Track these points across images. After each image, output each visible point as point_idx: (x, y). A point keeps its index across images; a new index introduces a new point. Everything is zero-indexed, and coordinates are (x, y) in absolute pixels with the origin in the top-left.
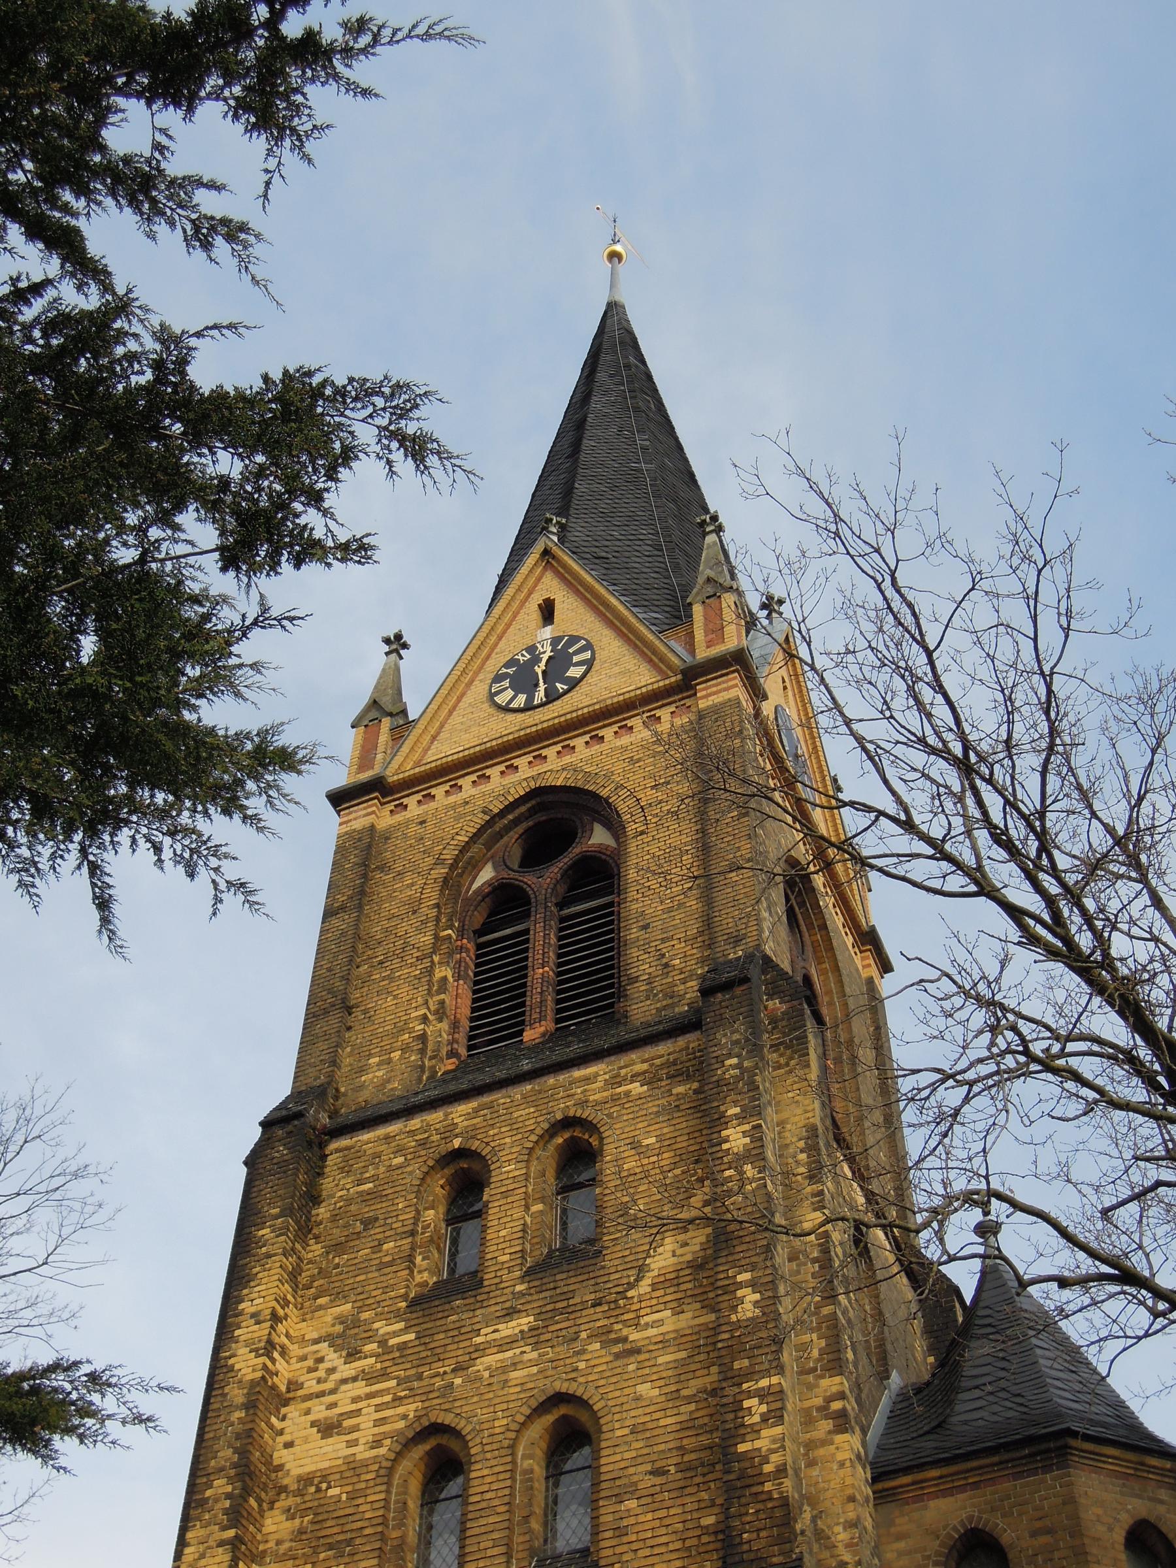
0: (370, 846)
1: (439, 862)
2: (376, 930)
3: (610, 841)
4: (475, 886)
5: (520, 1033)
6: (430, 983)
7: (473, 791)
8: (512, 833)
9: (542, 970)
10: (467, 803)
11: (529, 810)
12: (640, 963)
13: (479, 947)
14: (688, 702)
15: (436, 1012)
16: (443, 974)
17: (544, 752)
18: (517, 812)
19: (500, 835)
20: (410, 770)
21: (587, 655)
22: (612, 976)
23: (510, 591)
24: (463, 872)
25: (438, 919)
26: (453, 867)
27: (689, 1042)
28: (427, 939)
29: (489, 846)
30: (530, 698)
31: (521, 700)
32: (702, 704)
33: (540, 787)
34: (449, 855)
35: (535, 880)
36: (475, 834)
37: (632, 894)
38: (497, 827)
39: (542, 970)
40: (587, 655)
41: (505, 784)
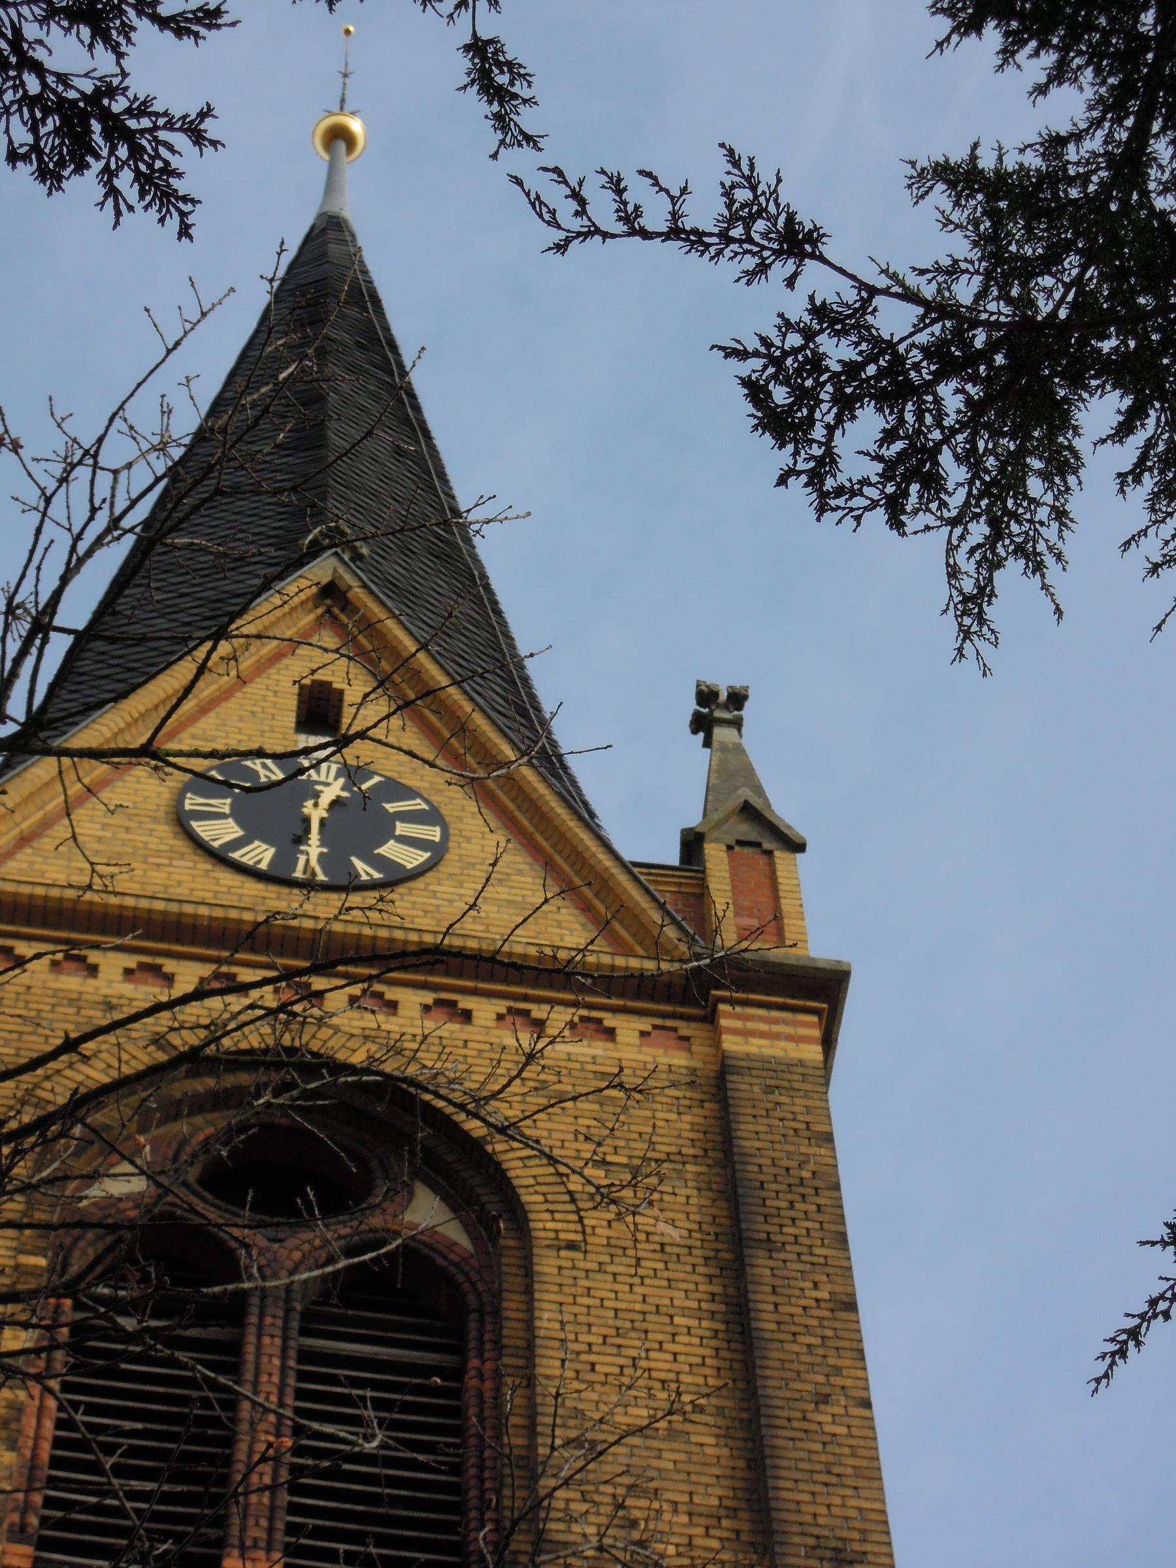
8: (198, 1120)
37: (548, 1366)
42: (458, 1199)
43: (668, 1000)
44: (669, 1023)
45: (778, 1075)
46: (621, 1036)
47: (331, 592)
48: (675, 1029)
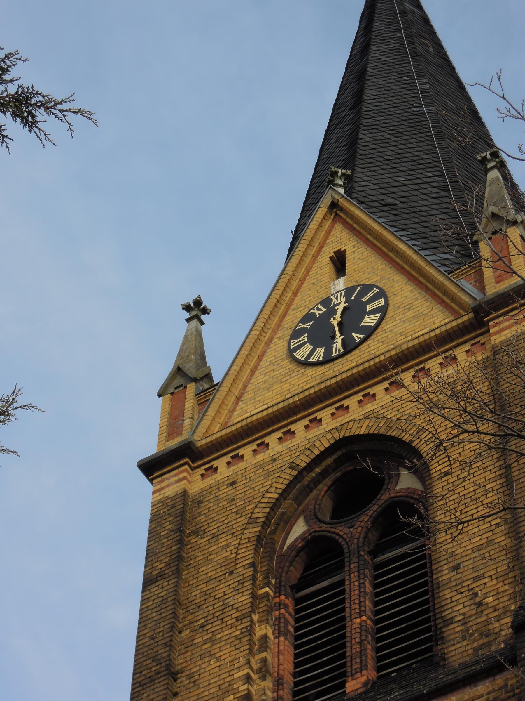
0: (183, 512)
1: (252, 521)
2: (196, 594)
3: (418, 486)
4: (289, 542)
5: (343, 685)
6: (251, 642)
7: (280, 448)
8: (320, 486)
9: (359, 620)
10: (274, 460)
11: (335, 461)
12: (454, 604)
13: (298, 601)
14: (482, 339)
15: (259, 671)
16: (263, 632)
17: (346, 403)
18: (324, 464)
19: (309, 489)
20: (218, 432)
21: (381, 302)
22: (428, 620)
23: (301, 247)
24: (276, 529)
25: (254, 578)
26: (265, 524)
27: (507, 679)
28: (245, 598)
30: (328, 351)
31: (320, 353)
32: (497, 339)
33: (344, 438)
34: (261, 513)
35: (346, 530)
36: (284, 490)
38: (306, 481)
39: (359, 620)
40: (381, 302)
41: (309, 438)
43: (475, 329)
44: (476, 340)
46: (459, 358)
48: (479, 342)
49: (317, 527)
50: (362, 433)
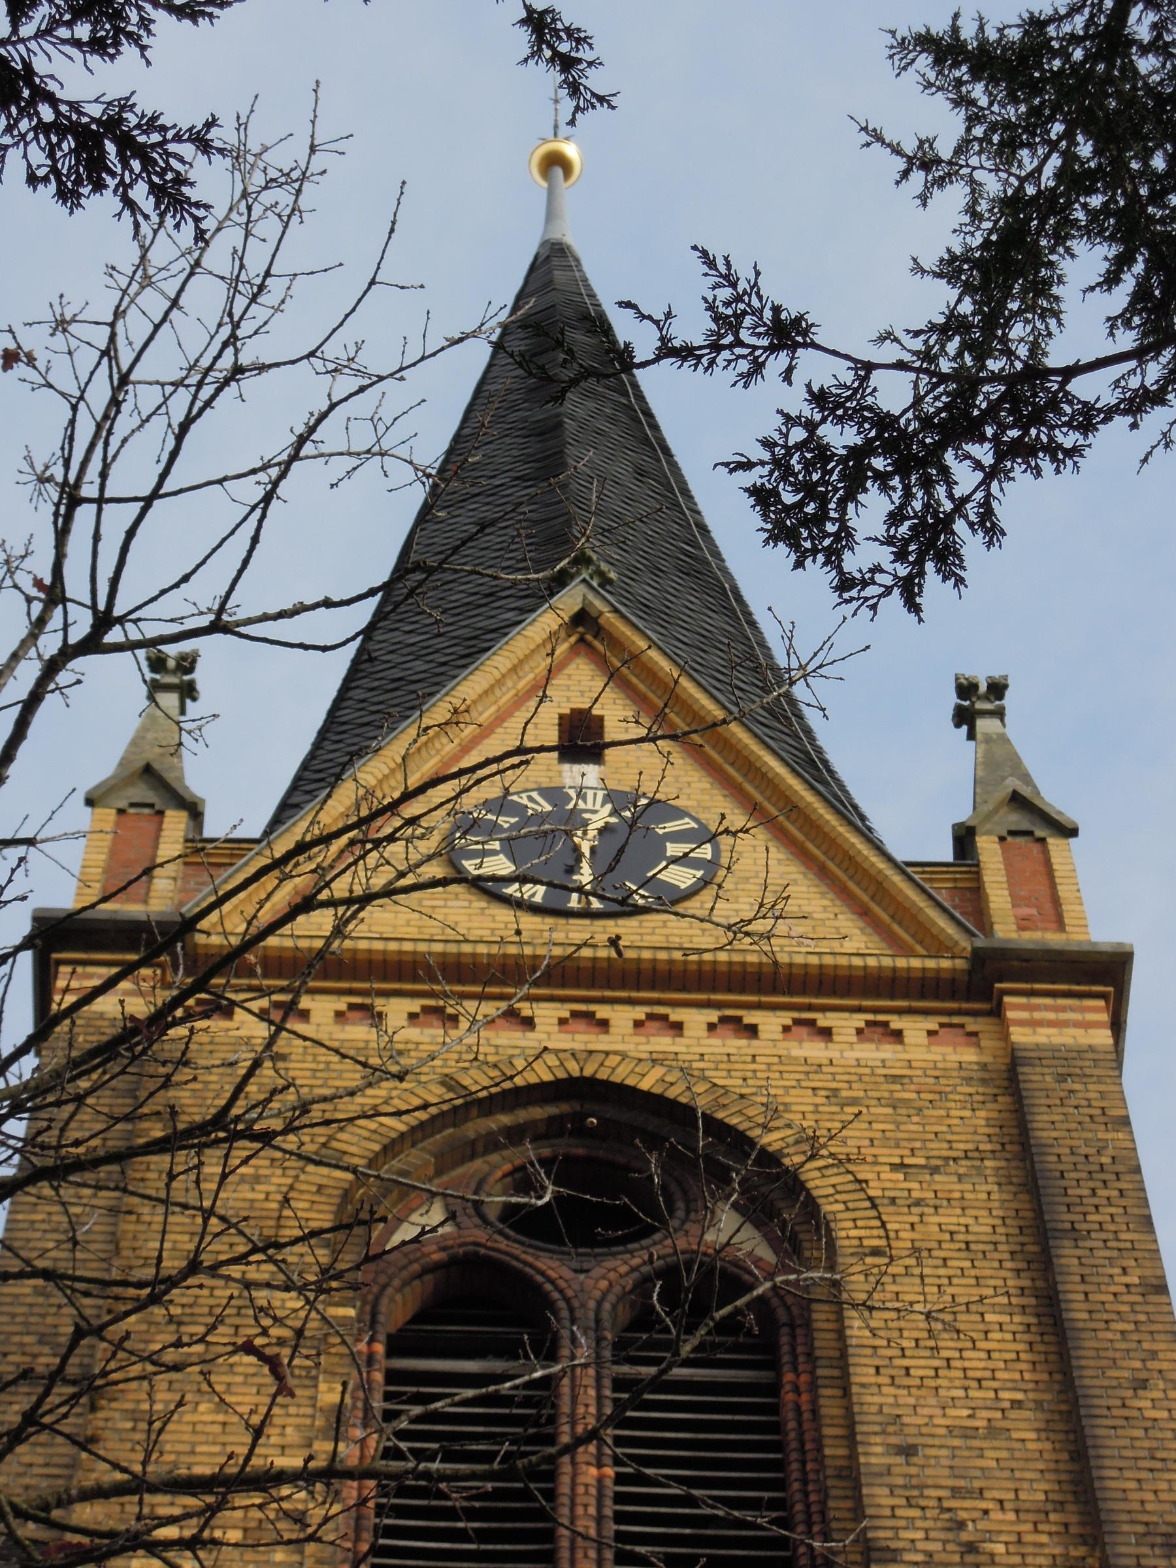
8: (494, 1158)
11: (551, 1119)
18: (523, 1115)
19: (471, 1150)
29: (445, 1162)
33: (592, 1082)
35: (568, 1274)
37: (862, 1373)
42: (757, 1211)
43: (953, 997)
44: (956, 1020)
45: (1069, 1063)
46: (909, 1037)
47: (582, 619)
48: (962, 1026)
49: (481, 1235)
50: (645, 1085)
